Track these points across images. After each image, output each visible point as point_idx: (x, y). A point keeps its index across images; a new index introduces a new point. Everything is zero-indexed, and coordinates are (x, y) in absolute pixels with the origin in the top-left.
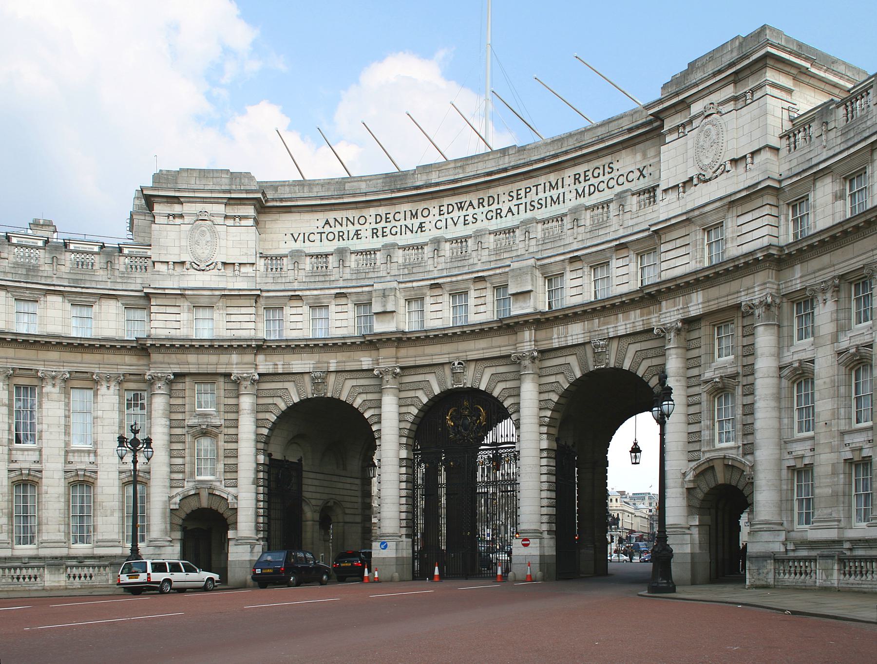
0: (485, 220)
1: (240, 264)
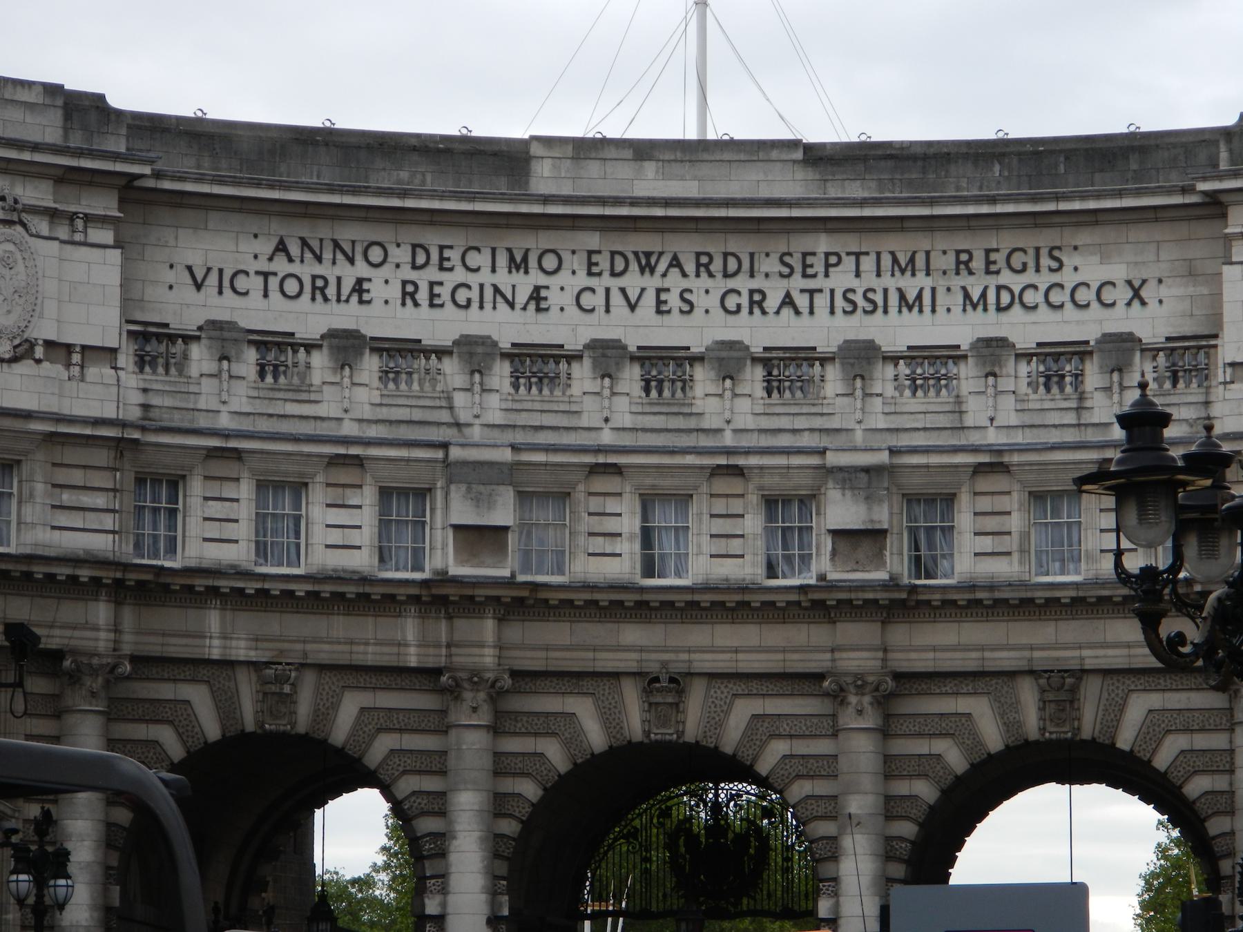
0: (717, 312)
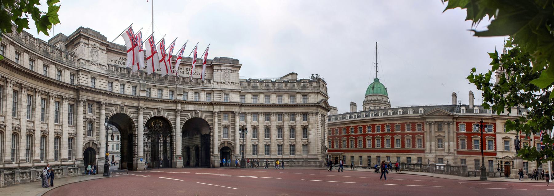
1: (103, 65)
